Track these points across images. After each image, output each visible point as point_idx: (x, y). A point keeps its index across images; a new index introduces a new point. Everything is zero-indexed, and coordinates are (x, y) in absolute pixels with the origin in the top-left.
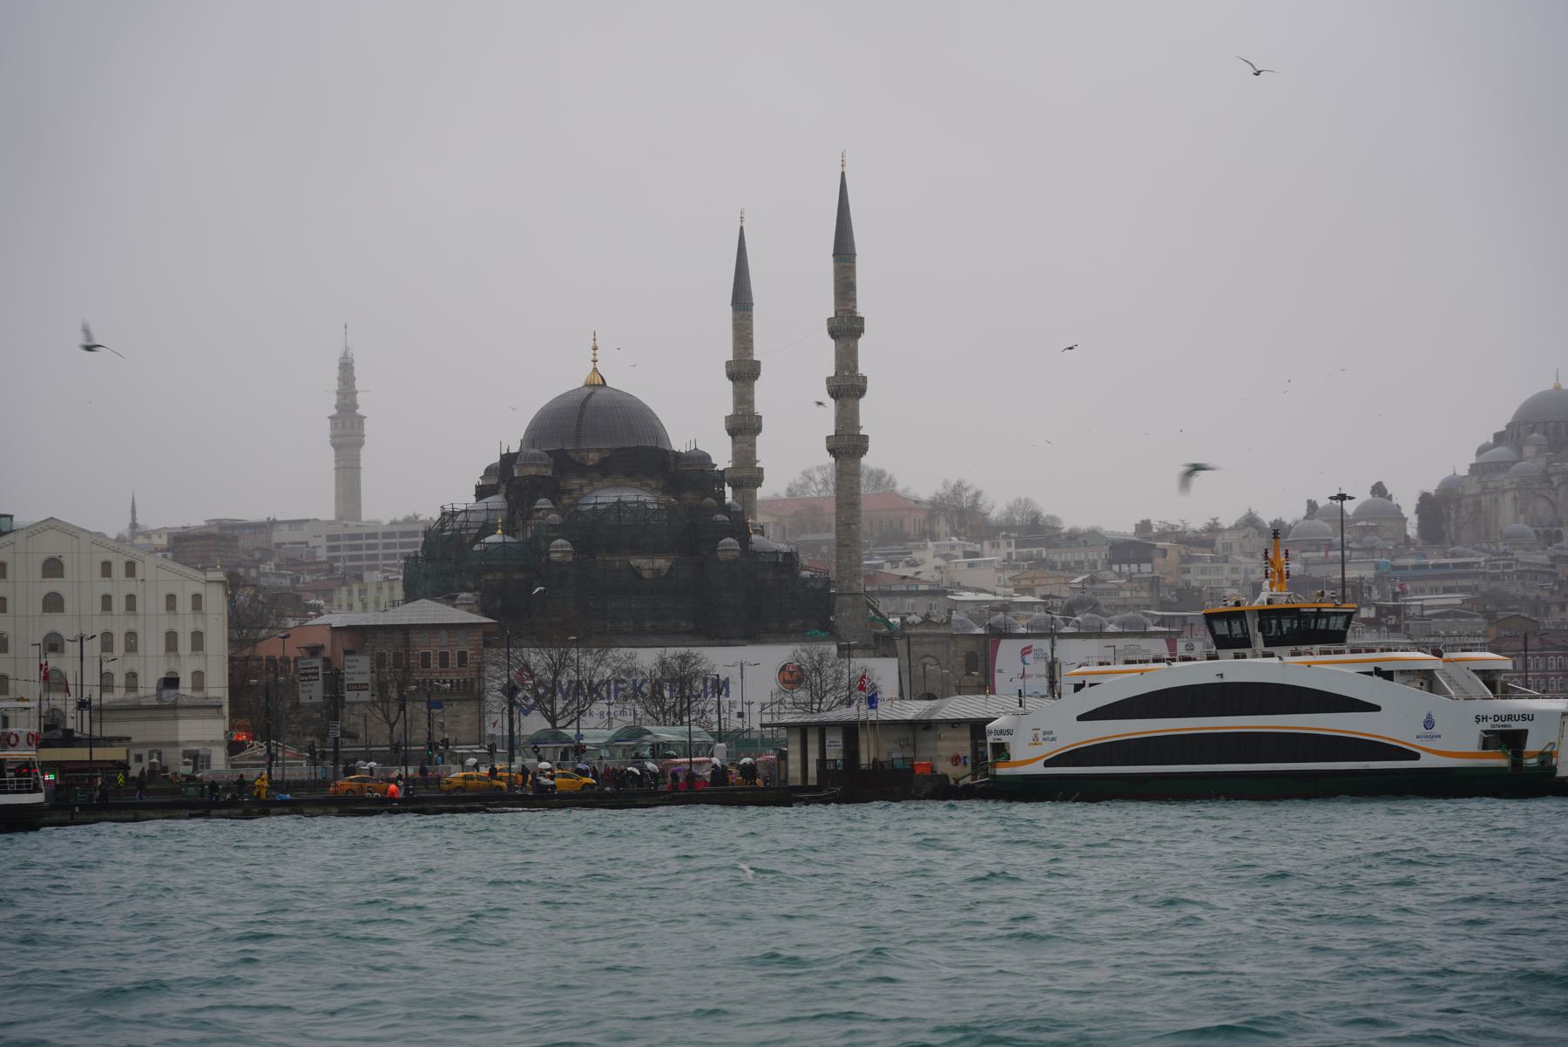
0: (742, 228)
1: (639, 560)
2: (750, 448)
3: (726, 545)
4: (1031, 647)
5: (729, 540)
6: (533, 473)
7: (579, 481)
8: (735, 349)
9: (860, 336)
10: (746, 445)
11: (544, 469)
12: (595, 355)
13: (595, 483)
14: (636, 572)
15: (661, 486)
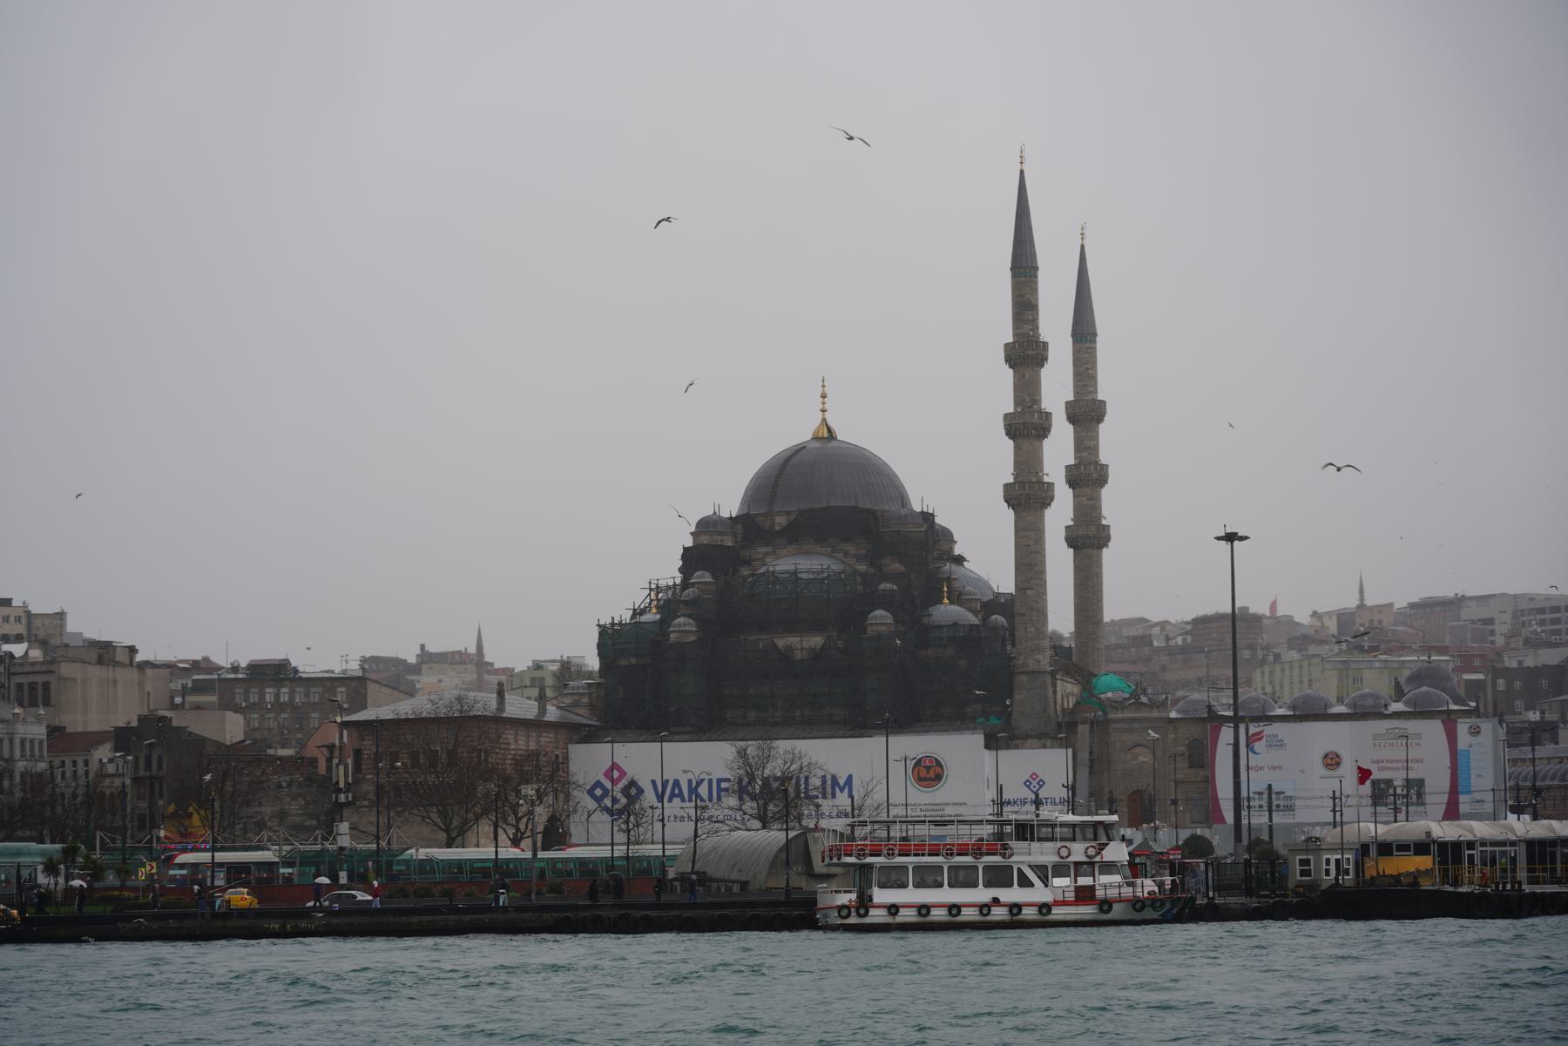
0: (1083, 247)
1: (791, 639)
2: (1090, 502)
3: (876, 617)
4: (1261, 732)
5: (879, 612)
6: (705, 542)
7: (764, 549)
8: (1075, 386)
9: (1042, 366)
10: (1085, 499)
11: (719, 538)
12: (824, 403)
13: (779, 551)
14: (786, 656)
15: (863, 552)
